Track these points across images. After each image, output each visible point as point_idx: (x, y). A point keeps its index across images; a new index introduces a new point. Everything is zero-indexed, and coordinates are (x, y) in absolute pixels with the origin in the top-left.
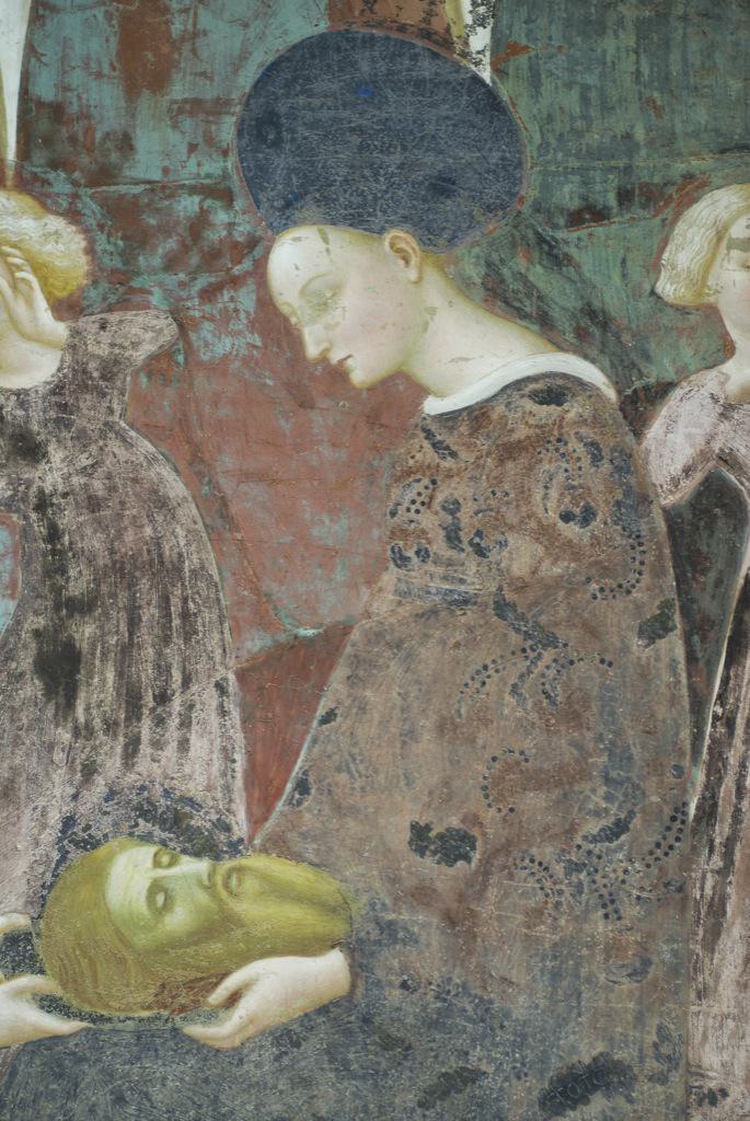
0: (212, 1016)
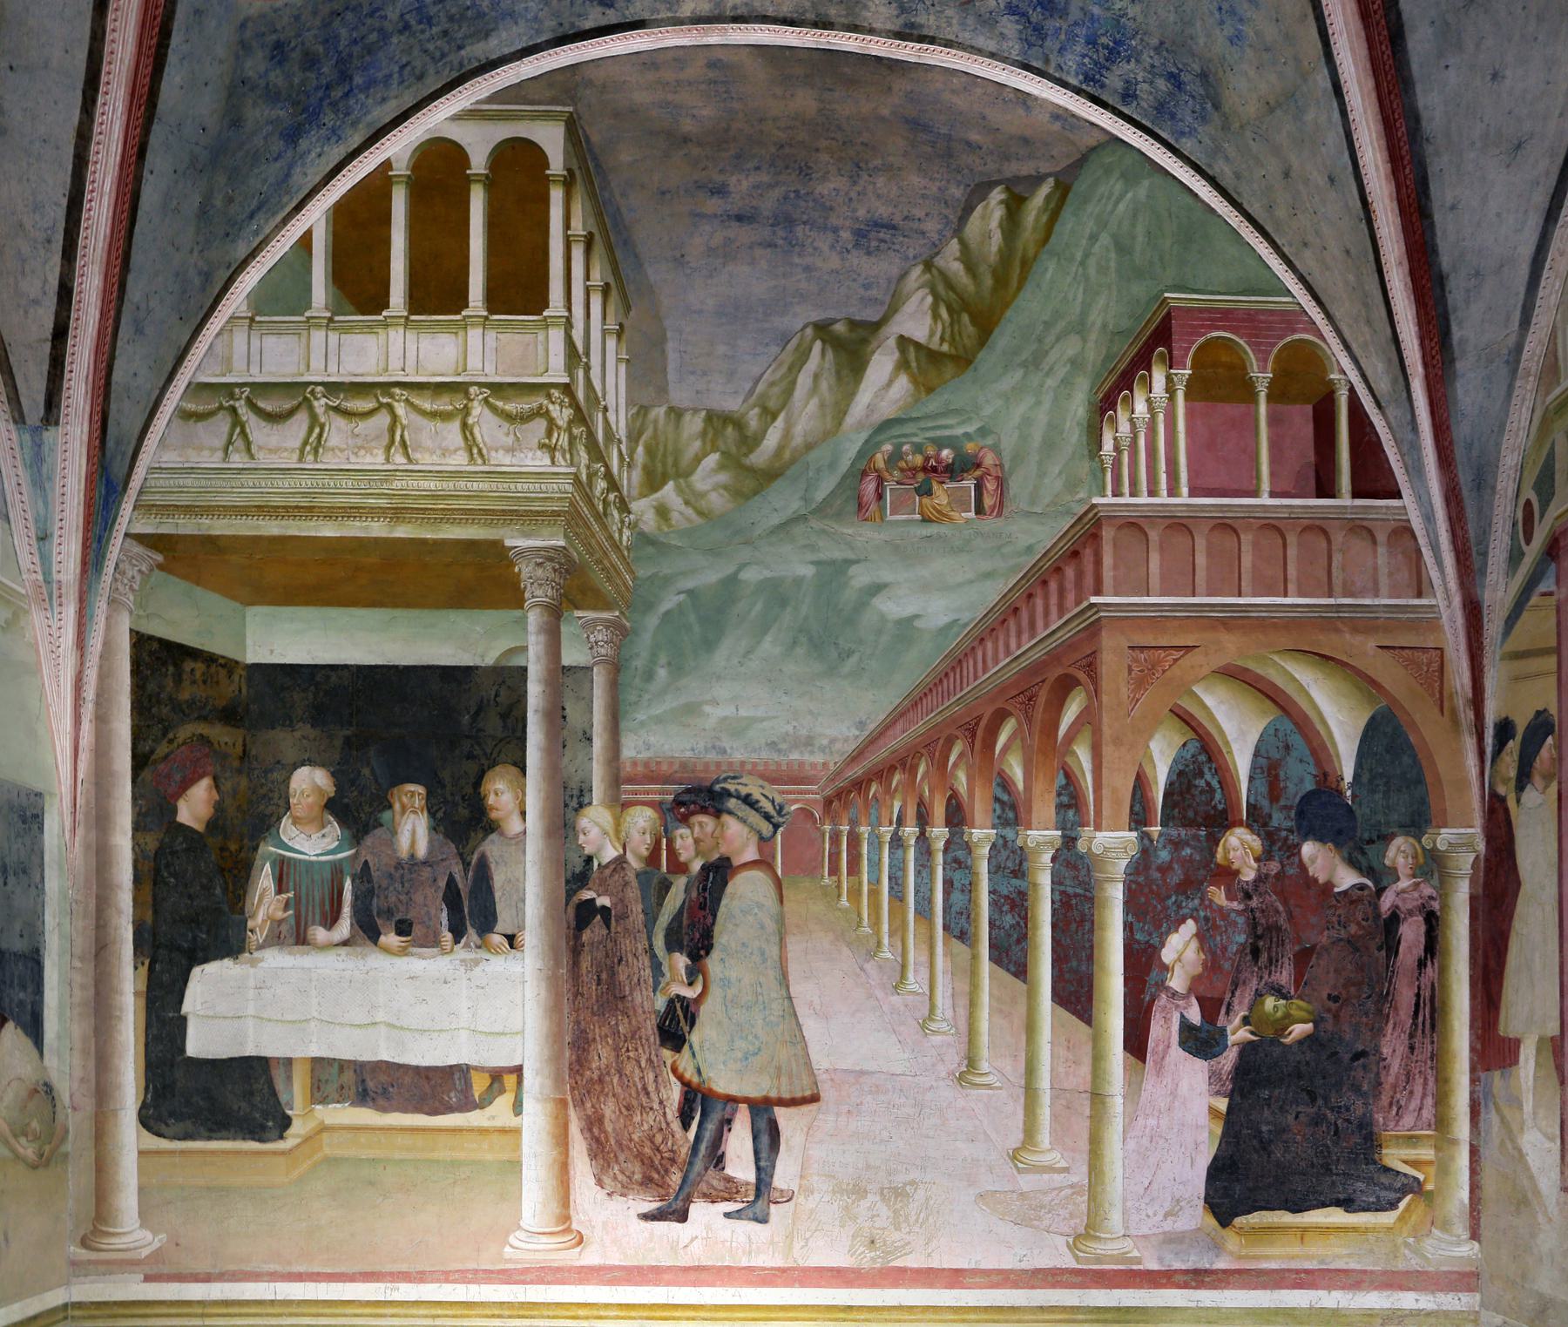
0: (1286, 1037)
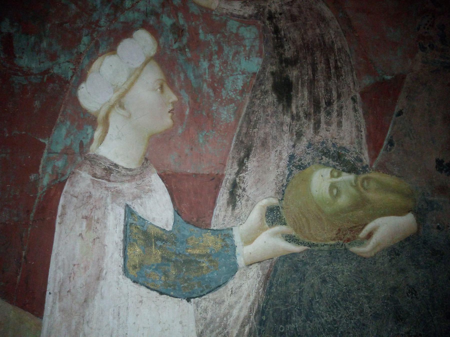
0: (361, 243)
